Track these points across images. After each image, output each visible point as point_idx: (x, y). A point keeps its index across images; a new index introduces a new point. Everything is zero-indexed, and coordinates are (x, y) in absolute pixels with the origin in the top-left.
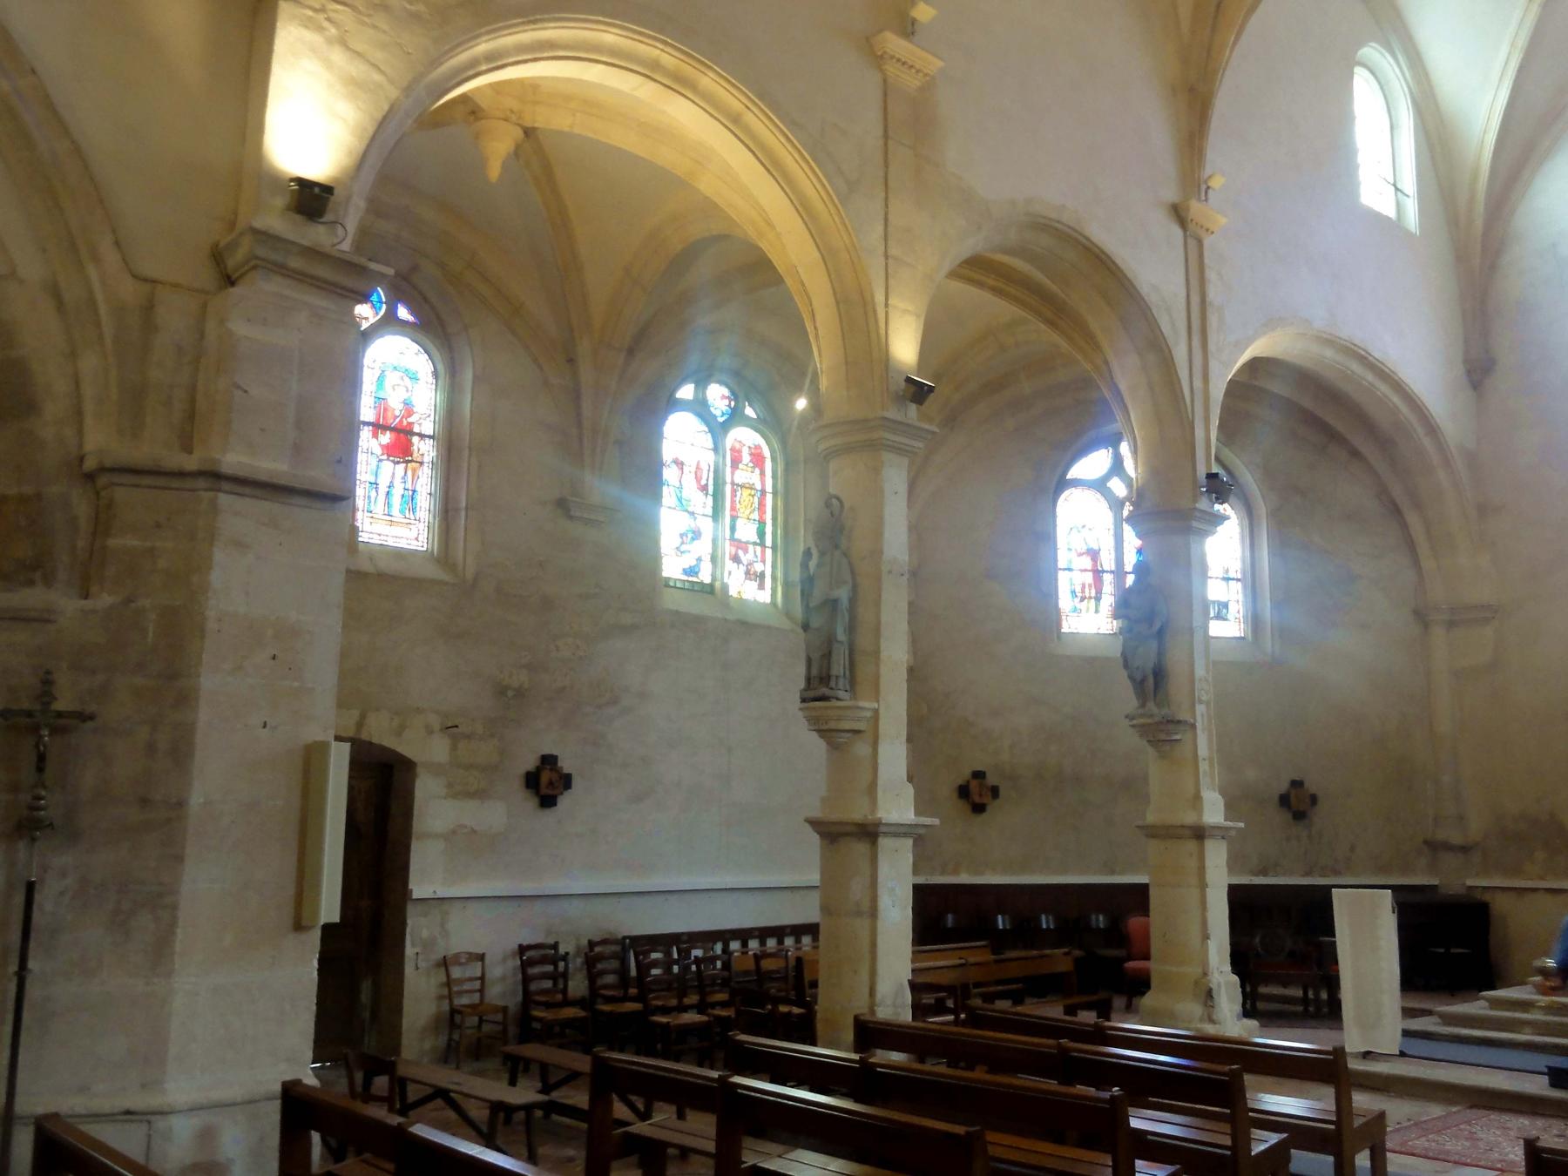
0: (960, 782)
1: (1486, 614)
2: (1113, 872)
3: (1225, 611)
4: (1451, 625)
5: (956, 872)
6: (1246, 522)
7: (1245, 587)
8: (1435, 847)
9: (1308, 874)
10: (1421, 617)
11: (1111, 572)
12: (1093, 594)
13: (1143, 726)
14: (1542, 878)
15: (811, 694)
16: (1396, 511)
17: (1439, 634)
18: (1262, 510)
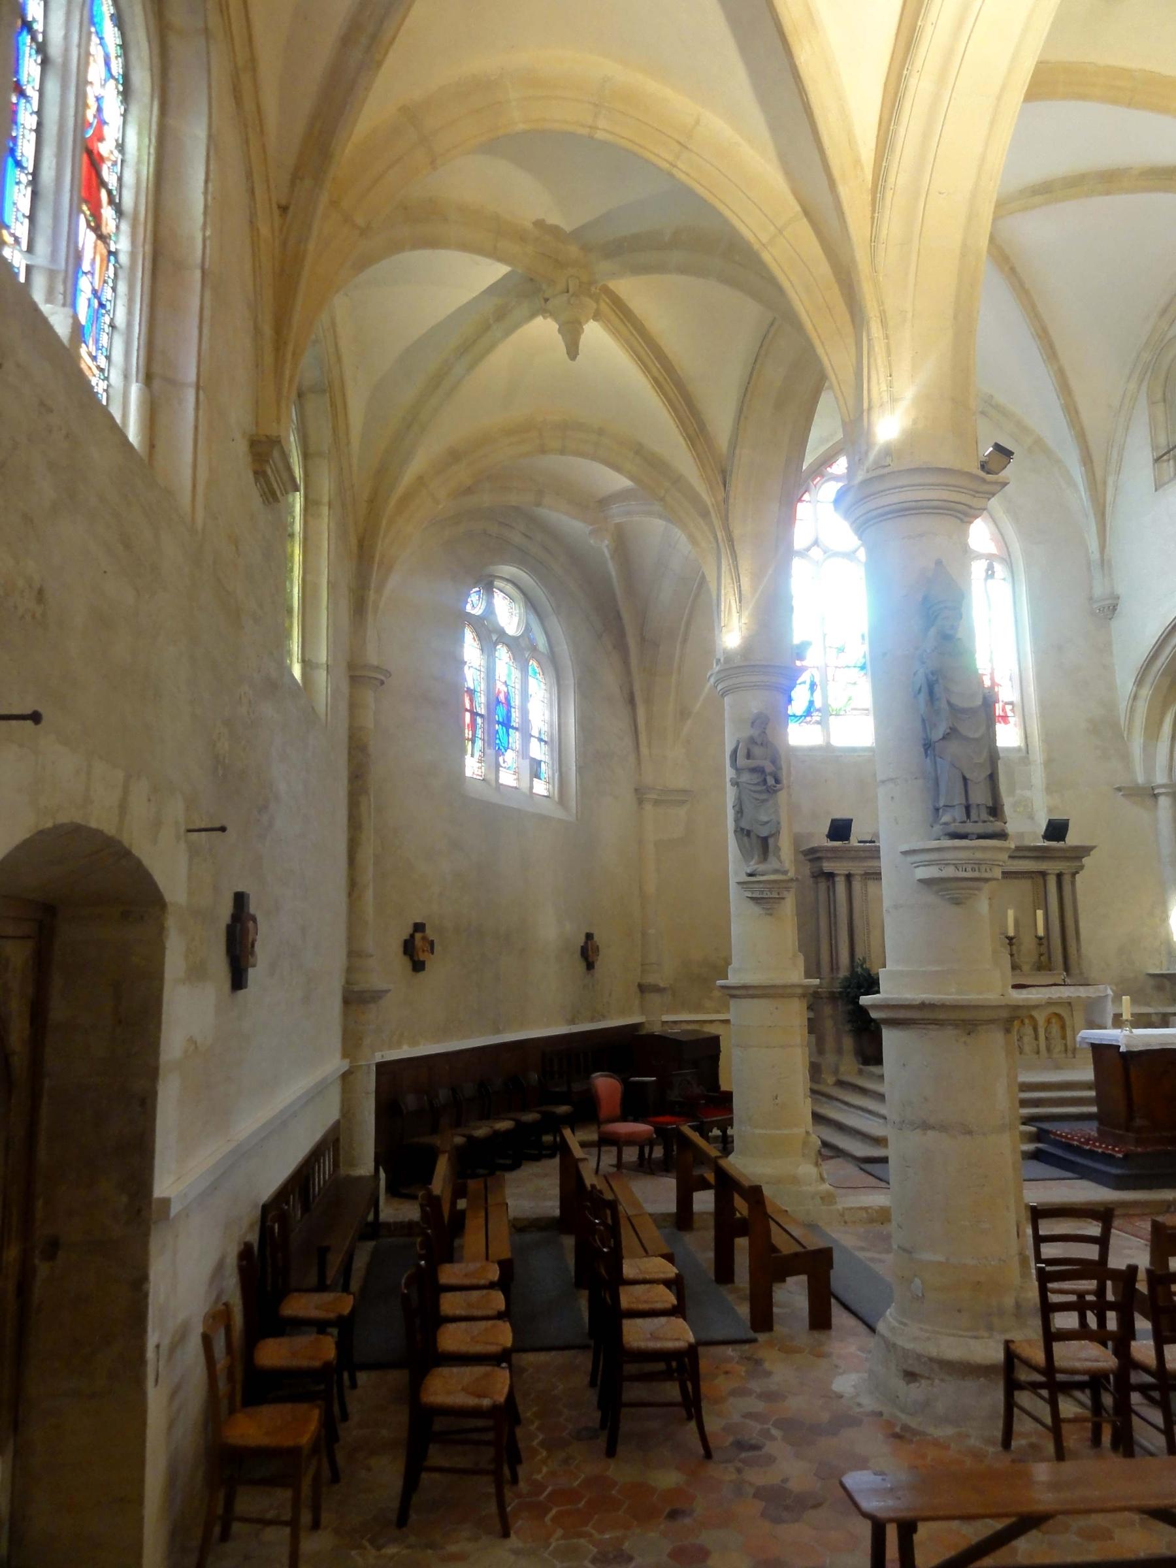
0: (406, 936)
1: (682, 797)
2: (498, 1031)
3: (539, 769)
4: (656, 803)
5: (399, 1045)
6: (555, 690)
7: (552, 750)
8: (642, 988)
9: (592, 1020)
10: (640, 794)
11: (481, 716)
12: (470, 737)
13: (775, 881)
14: (718, 1012)
15: (969, 828)
16: (631, 701)
17: (648, 807)
18: (570, 682)
